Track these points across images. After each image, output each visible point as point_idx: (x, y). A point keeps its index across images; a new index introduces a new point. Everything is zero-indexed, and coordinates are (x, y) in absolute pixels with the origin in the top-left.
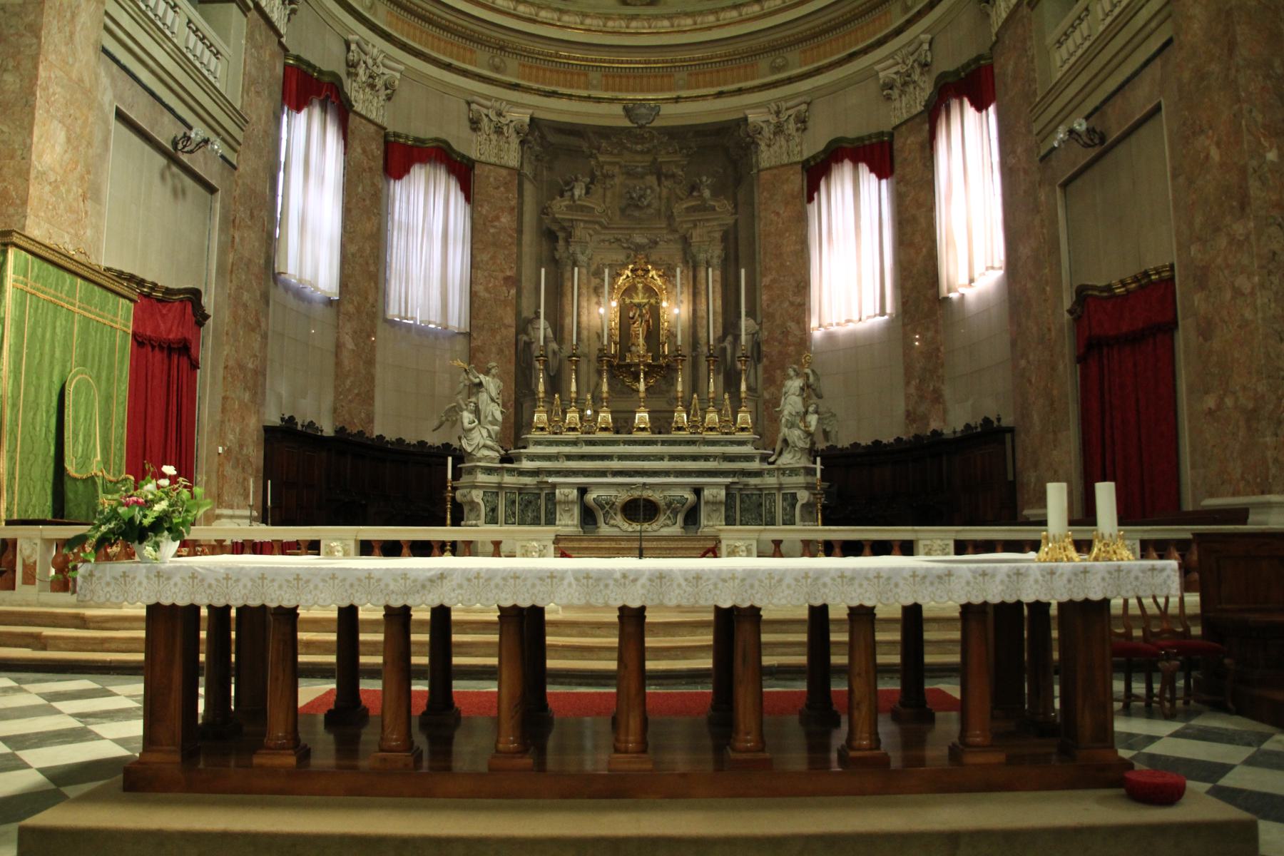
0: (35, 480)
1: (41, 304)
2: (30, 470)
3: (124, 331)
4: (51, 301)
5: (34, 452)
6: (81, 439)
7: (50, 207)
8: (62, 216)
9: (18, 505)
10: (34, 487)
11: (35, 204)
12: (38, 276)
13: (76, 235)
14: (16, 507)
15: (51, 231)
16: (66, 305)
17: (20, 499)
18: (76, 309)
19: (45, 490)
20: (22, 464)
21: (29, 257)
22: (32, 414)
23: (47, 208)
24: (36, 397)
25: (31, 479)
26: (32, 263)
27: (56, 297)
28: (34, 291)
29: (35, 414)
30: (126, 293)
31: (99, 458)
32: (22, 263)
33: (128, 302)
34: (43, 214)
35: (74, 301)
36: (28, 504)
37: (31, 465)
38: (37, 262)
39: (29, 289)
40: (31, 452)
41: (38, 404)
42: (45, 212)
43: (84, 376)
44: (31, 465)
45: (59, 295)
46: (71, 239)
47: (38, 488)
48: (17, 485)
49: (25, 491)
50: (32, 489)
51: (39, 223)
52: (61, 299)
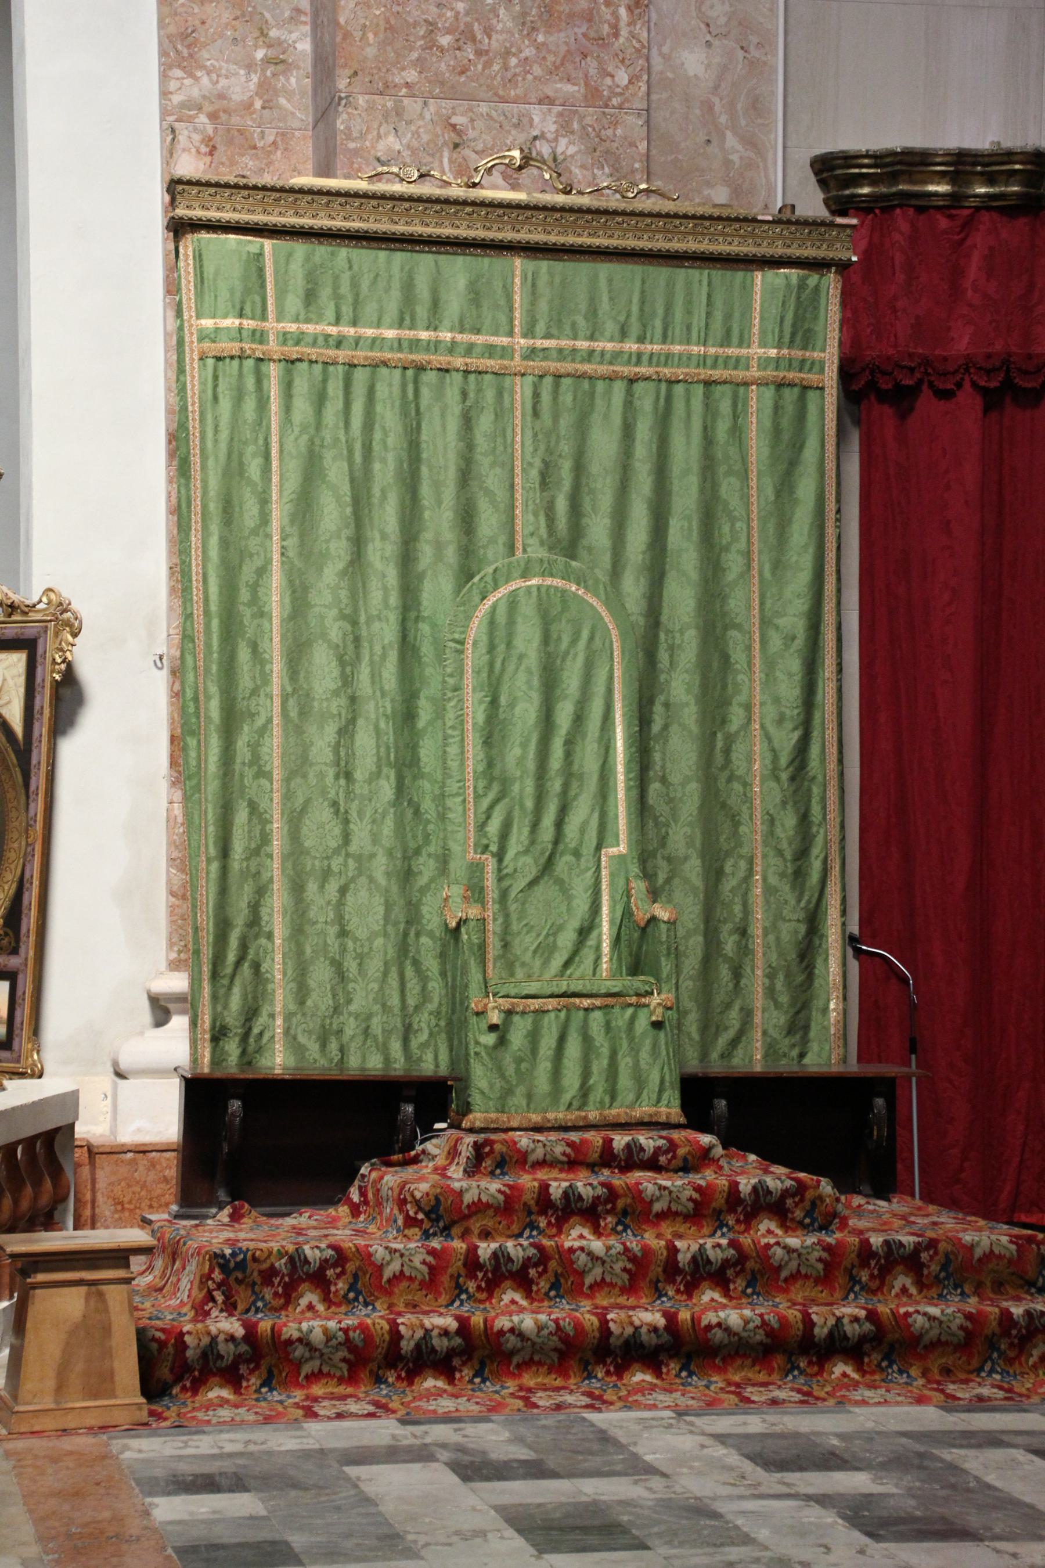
0: (362, 933)
1: (335, 389)
2: (340, 904)
3: (780, 385)
4: (385, 363)
5: (353, 848)
6: (525, 788)
7: (445, 40)
8: (508, 53)
9: (288, 1017)
10: (361, 958)
11: (370, 52)
12: (310, 297)
13: (593, 95)
14: (279, 1021)
15: (457, 120)
16: (459, 362)
17: (301, 993)
18: (517, 362)
19: (416, 963)
20: (297, 888)
21: (268, 245)
22: (331, 730)
23: (431, 44)
24: (347, 680)
25: (343, 933)
26: (283, 263)
27: (415, 344)
28: (294, 352)
29: (347, 731)
30: (779, 250)
31: (622, 848)
32: (234, 272)
33: (794, 274)
34: (411, 75)
35: (504, 340)
36: (336, 1010)
37: (343, 891)
38: (300, 248)
39: (273, 346)
40: (336, 851)
41: (353, 699)
42: (420, 64)
43: (557, 582)
44: (343, 891)
45: (424, 335)
46: (565, 127)
47: (375, 966)
48: (278, 957)
49: (321, 974)
50: (351, 965)
51: (399, 112)
52: (435, 346)
